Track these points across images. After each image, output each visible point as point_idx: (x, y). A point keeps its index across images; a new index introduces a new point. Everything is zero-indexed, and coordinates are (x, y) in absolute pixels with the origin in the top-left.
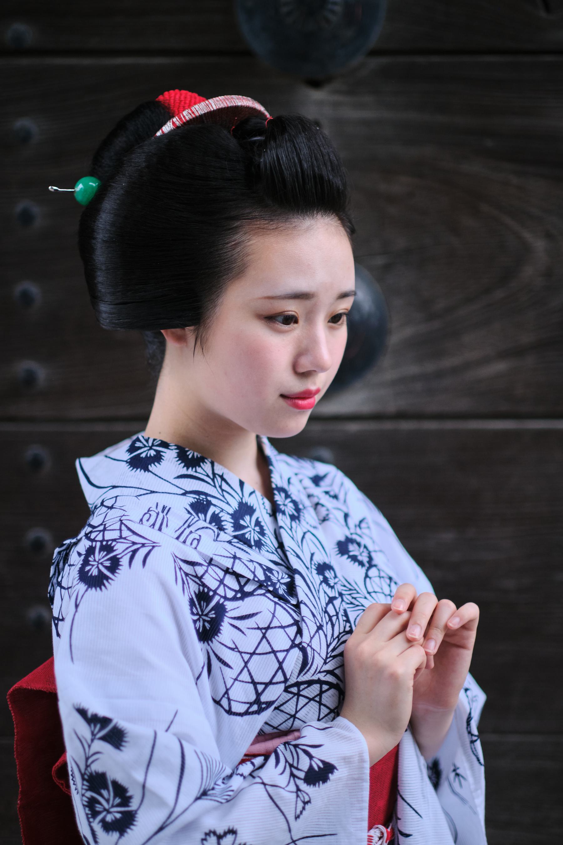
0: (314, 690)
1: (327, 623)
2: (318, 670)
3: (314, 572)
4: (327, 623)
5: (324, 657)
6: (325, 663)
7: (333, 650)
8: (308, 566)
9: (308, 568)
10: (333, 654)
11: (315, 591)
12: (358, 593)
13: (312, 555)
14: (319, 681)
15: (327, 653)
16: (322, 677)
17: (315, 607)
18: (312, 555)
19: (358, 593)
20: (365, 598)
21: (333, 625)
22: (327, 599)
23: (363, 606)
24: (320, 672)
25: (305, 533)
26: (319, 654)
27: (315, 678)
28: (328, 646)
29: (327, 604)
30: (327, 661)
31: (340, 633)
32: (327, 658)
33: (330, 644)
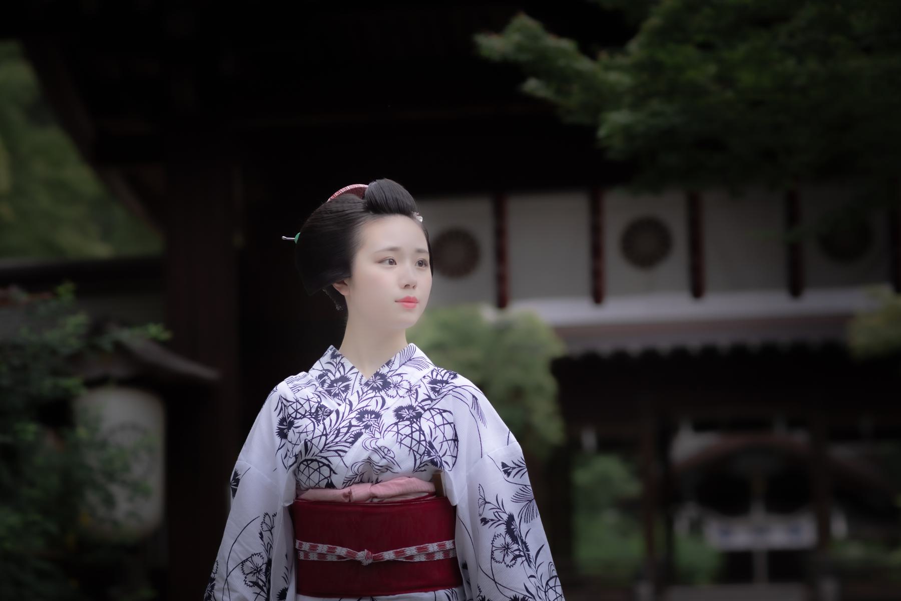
0: (315, 465)
1: (333, 434)
2: (315, 455)
3: (356, 412)
4: (333, 434)
5: (321, 449)
6: (321, 452)
7: (328, 447)
8: (353, 409)
9: (351, 409)
10: (328, 449)
11: (342, 419)
12: (379, 429)
13: (367, 406)
14: (316, 460)
15: (324, 447)
16: (318, 458)
17: (331, 425)
18: (367, 406)
19: (379, 429)
20: (380, 433)
21: (337, 436)
22: (348, 424)
23: (374, 435)
24: (316, 456)
25: (375, 396)
26: (317, 447)
27: (314, 458)
28: (325, 445)
29: (343, 427)
30: (323, 451)
31: (340, 441)
32: (322, 450)
33: (328, 444)
